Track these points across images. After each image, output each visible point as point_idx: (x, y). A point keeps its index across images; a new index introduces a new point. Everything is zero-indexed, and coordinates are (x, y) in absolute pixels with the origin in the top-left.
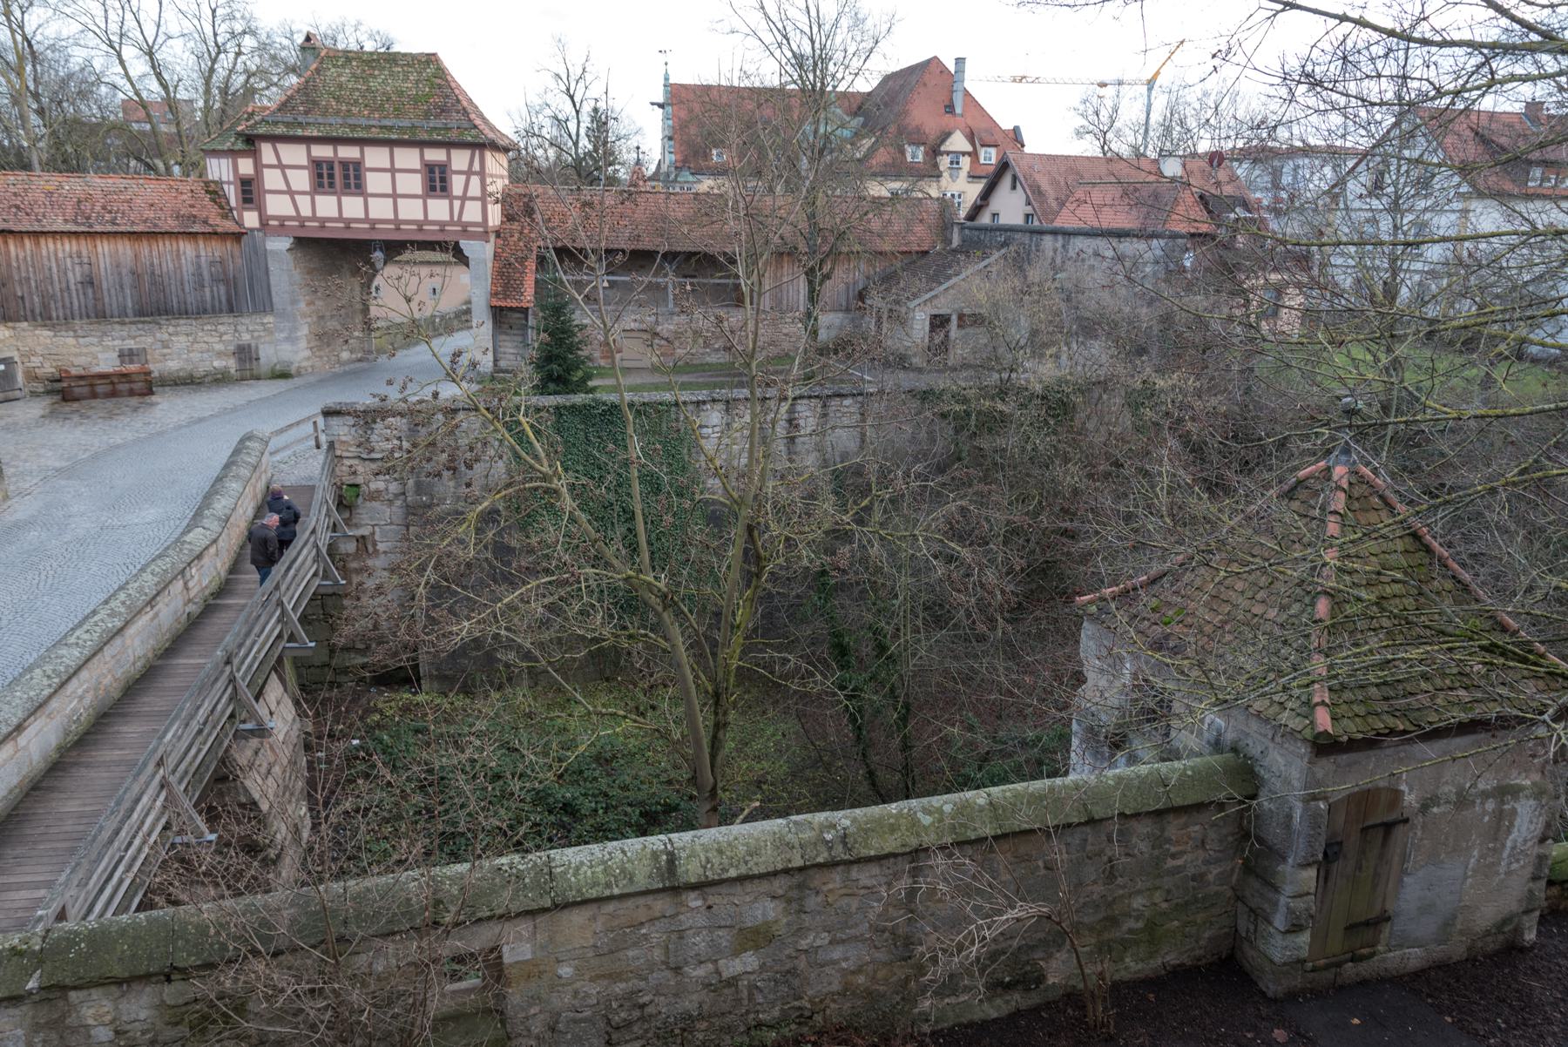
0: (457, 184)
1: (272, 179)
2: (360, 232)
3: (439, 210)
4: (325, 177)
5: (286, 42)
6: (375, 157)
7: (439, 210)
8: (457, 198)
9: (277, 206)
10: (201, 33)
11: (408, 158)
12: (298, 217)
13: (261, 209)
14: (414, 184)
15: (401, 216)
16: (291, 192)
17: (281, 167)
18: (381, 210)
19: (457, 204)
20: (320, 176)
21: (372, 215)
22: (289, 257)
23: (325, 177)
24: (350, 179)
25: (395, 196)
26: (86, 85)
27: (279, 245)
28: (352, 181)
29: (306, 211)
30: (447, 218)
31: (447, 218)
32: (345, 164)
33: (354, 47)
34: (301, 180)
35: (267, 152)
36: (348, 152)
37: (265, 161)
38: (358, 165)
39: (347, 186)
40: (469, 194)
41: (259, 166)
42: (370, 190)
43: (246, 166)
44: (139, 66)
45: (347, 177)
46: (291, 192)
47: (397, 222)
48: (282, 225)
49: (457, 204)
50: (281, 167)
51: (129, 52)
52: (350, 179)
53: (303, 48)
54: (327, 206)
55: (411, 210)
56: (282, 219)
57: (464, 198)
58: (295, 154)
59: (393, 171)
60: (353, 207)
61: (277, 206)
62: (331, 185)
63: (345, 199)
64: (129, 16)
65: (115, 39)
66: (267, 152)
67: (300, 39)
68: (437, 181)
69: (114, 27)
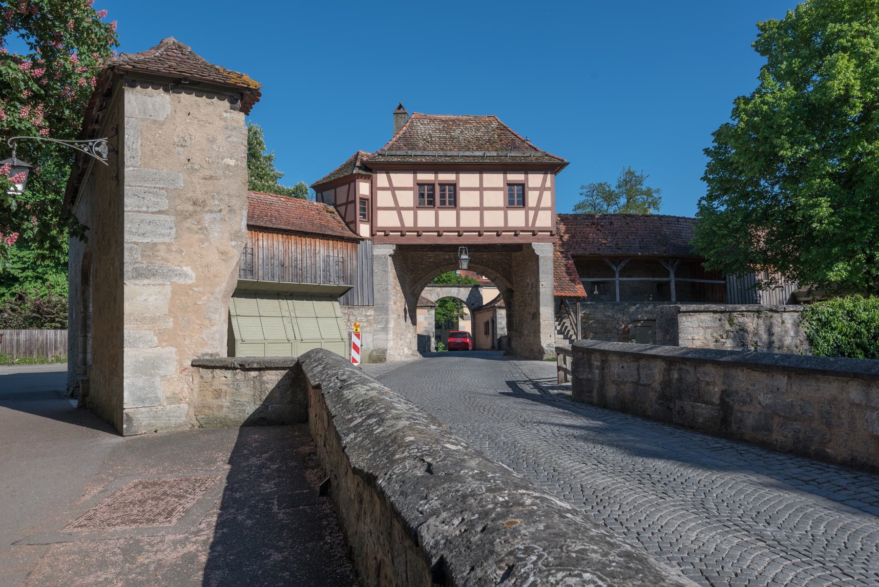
0: (532, 198)
1: (384, 199)
2: (451, 238)
3: (517, 218)
4: (427, 197)
6: (467, 180)
7: (517, 218)
8: (532, 209)
9: (386, 219)
11: (495, 180)
13: (372, 221)
14: (497, 199)
16: (398, 209)
17: (392, 189)
18: (470, 220)
19: (531, 213)
20: (422, 195)
22: (390, 261)
23: (427, 197)
24: (449, 198)
25: (481, 209)
27: (386, 251)
29: (409, 223)
30: (523, 225)
31: (523, 225)
32: (443, 185)
34: (407, 199)
36: (444, 177)
37: (379, 185)
38: (454, 185)
39: (443, 203)
40: (542, 205)
45: (443, 196)
46: (398, 209)
48: (386, 231)
49: (531, 213)
50: (392, 189)
52: (449, 198)
54: (426, 218)
55: (494, 220)
57: (537, 209)
58: (404, 179)
59: (481, 189)
60: (447, 218)
61: (386, 219)
66: (381, 179)
68: (517, 197)
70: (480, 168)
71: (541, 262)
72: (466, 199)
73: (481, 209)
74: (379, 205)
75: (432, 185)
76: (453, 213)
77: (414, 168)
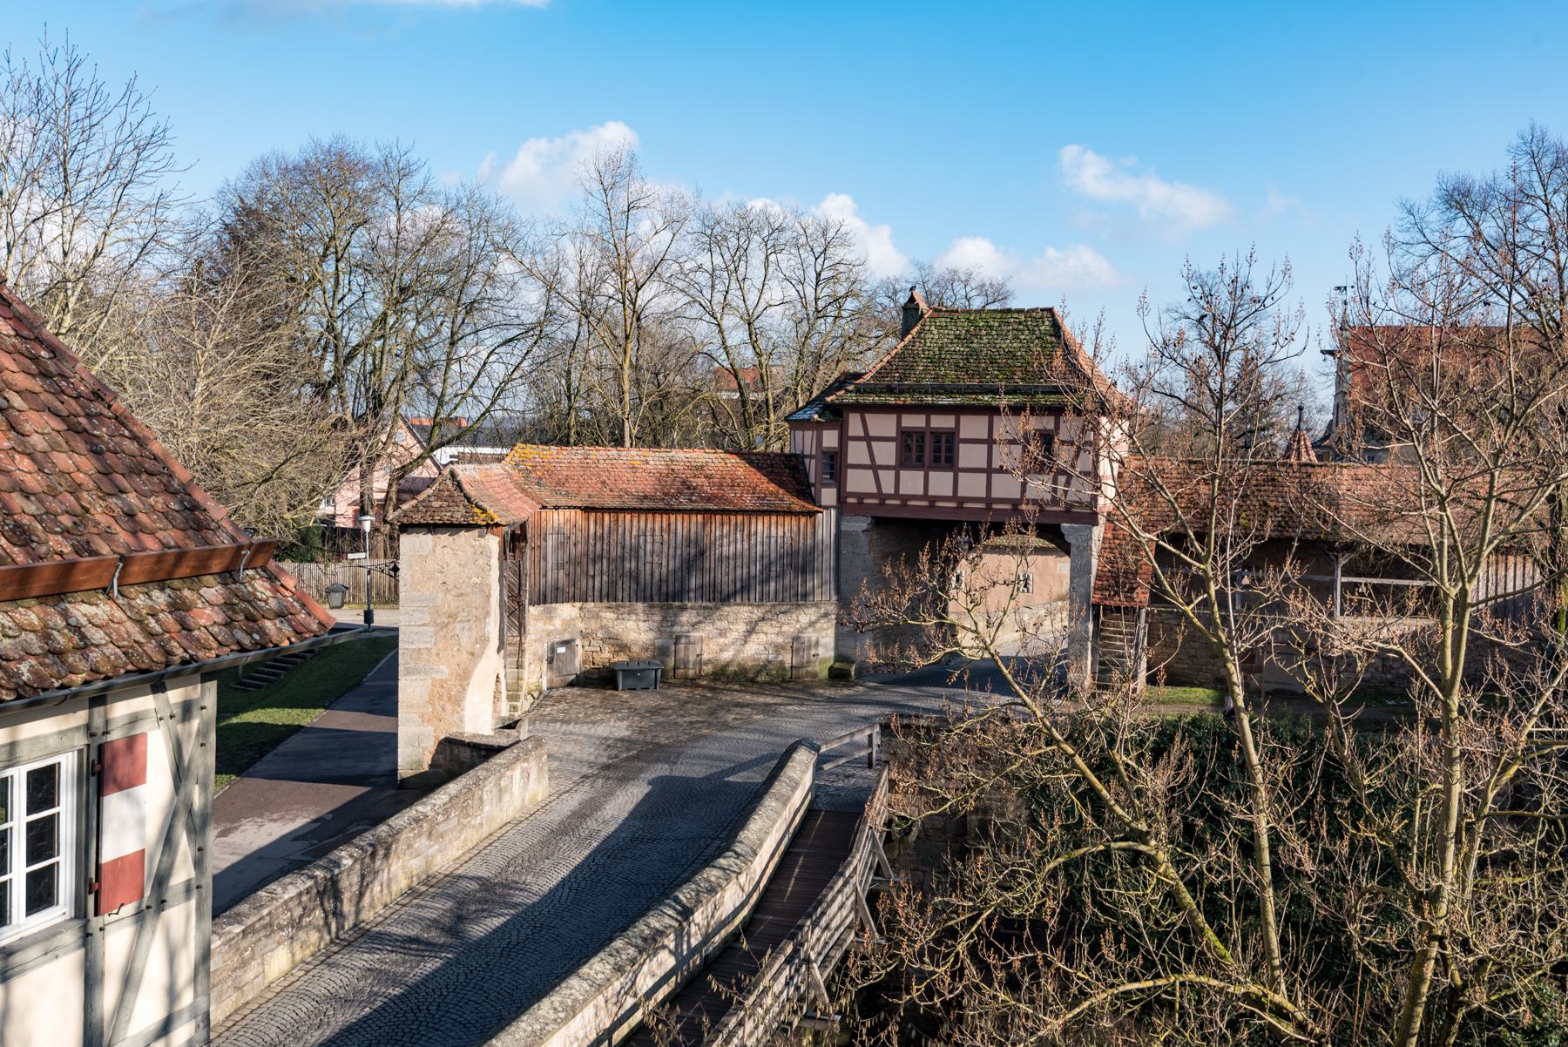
0: (1063, 456)
1: (857, 453)
5: (886, 301)
6: (972, 427)
10: (802, 298)
12: (880, 495)
15: (994, 495)
16: (874, 468)
17: (868, 439)
18: (972, 486)
21: (961, 493)
25: (989, 471)
26: (687, 355)
28: (943, 454)
29: (888, 488)
32: (937, 435)
33: (961, 304)
34: (887, 453)
35: (855, 424)
36: (942, 422)
39: (937, 459)
41: (844, 439)
42: (962, 464)
43: (830, 439)
44: (737, 336)
45: (937, 450)
46: (874, 468)
47: (989, 500)
50: (868, 439)
51: (729, 321)
53: (905, 309)
54: (912, 482)
55: (1006, 487)
56: (861, 496)
58: (883, 425)
60: (941, 483)
62: (920, 459)
63: (932, 474)
64: (734, 285)
65: (717, 309)
67: (903, 299)
69: (718, 297)
72: (970, 456)
73: (989, 471)
74: (850, 461)
75: (919, 434)
76: (948, 476)
77: (899, 410)
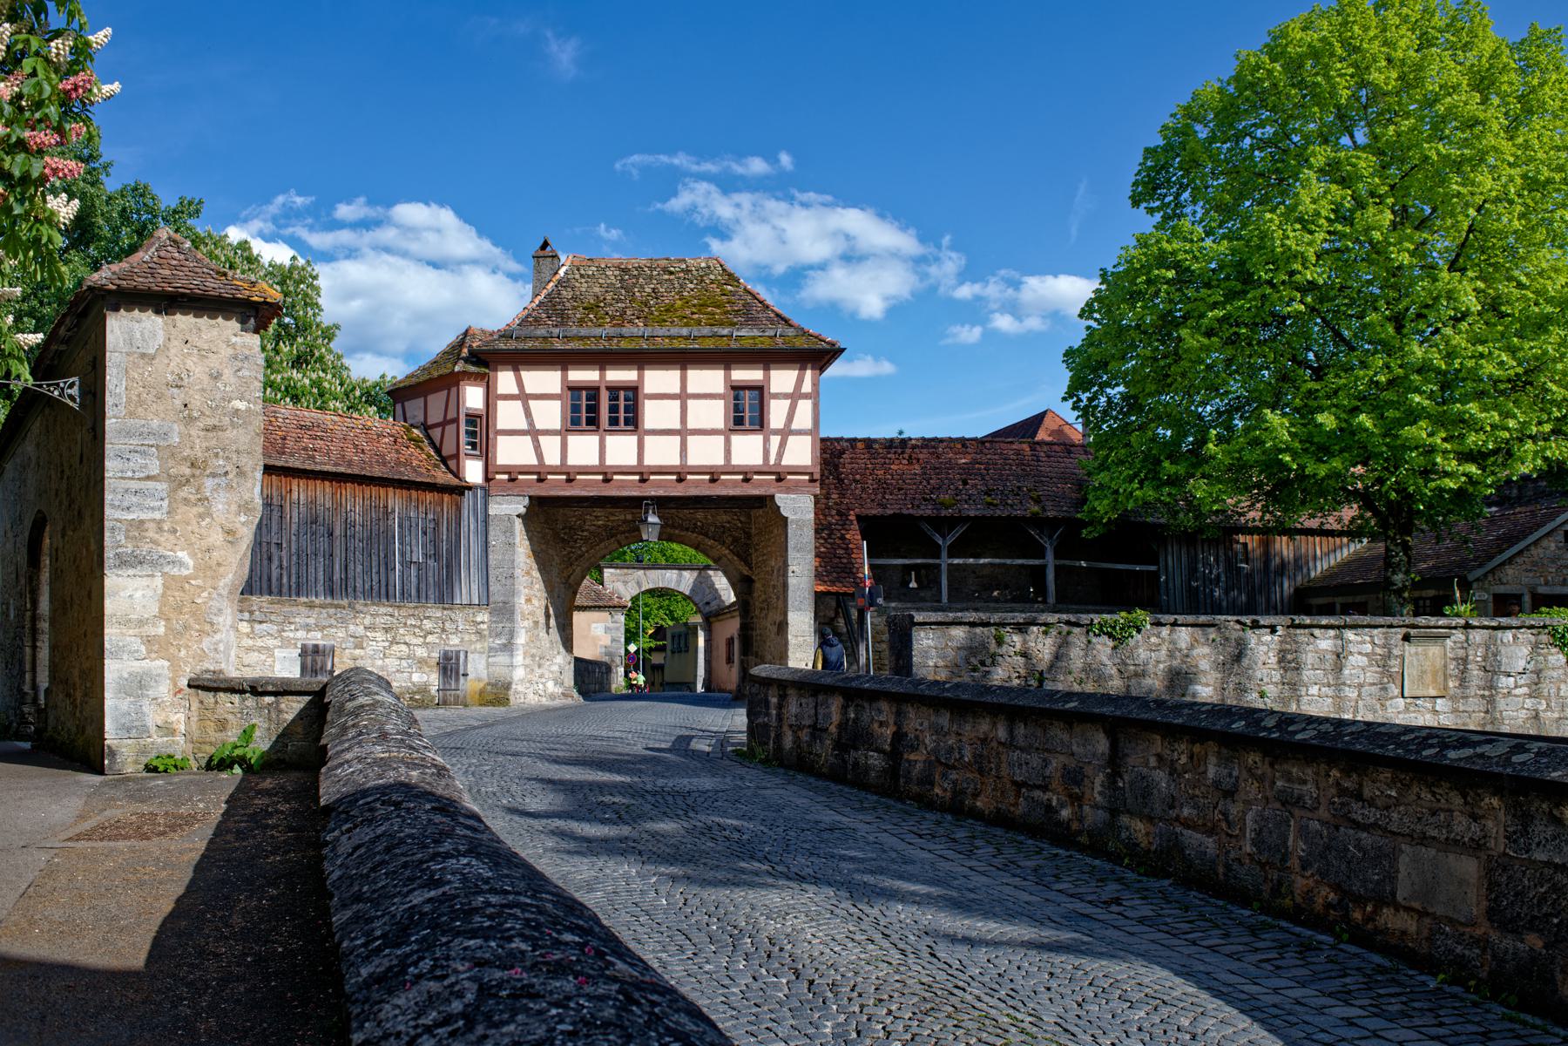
1: (508, 415)
3: (748, 450)
7: (748, 450)
8: (776, 432)
9: (512, 452)
14: (713, 414)
16: (534, 433)
18: (662, 452)
24: (625, 412)
25: (683, 432)
27: (509, 507)
34: (550, 414)
46: (534, 433)
49: (775, 440)
52: (625, 412)
54: (584, 450)
55: (707, 452)
57: (786, 433)
58: (545, 380)
59: (683, 396)
60: (621, 450)
61: (512, 452)
70: (683, 359)
71: (791, 529)
72: (655, 414)
